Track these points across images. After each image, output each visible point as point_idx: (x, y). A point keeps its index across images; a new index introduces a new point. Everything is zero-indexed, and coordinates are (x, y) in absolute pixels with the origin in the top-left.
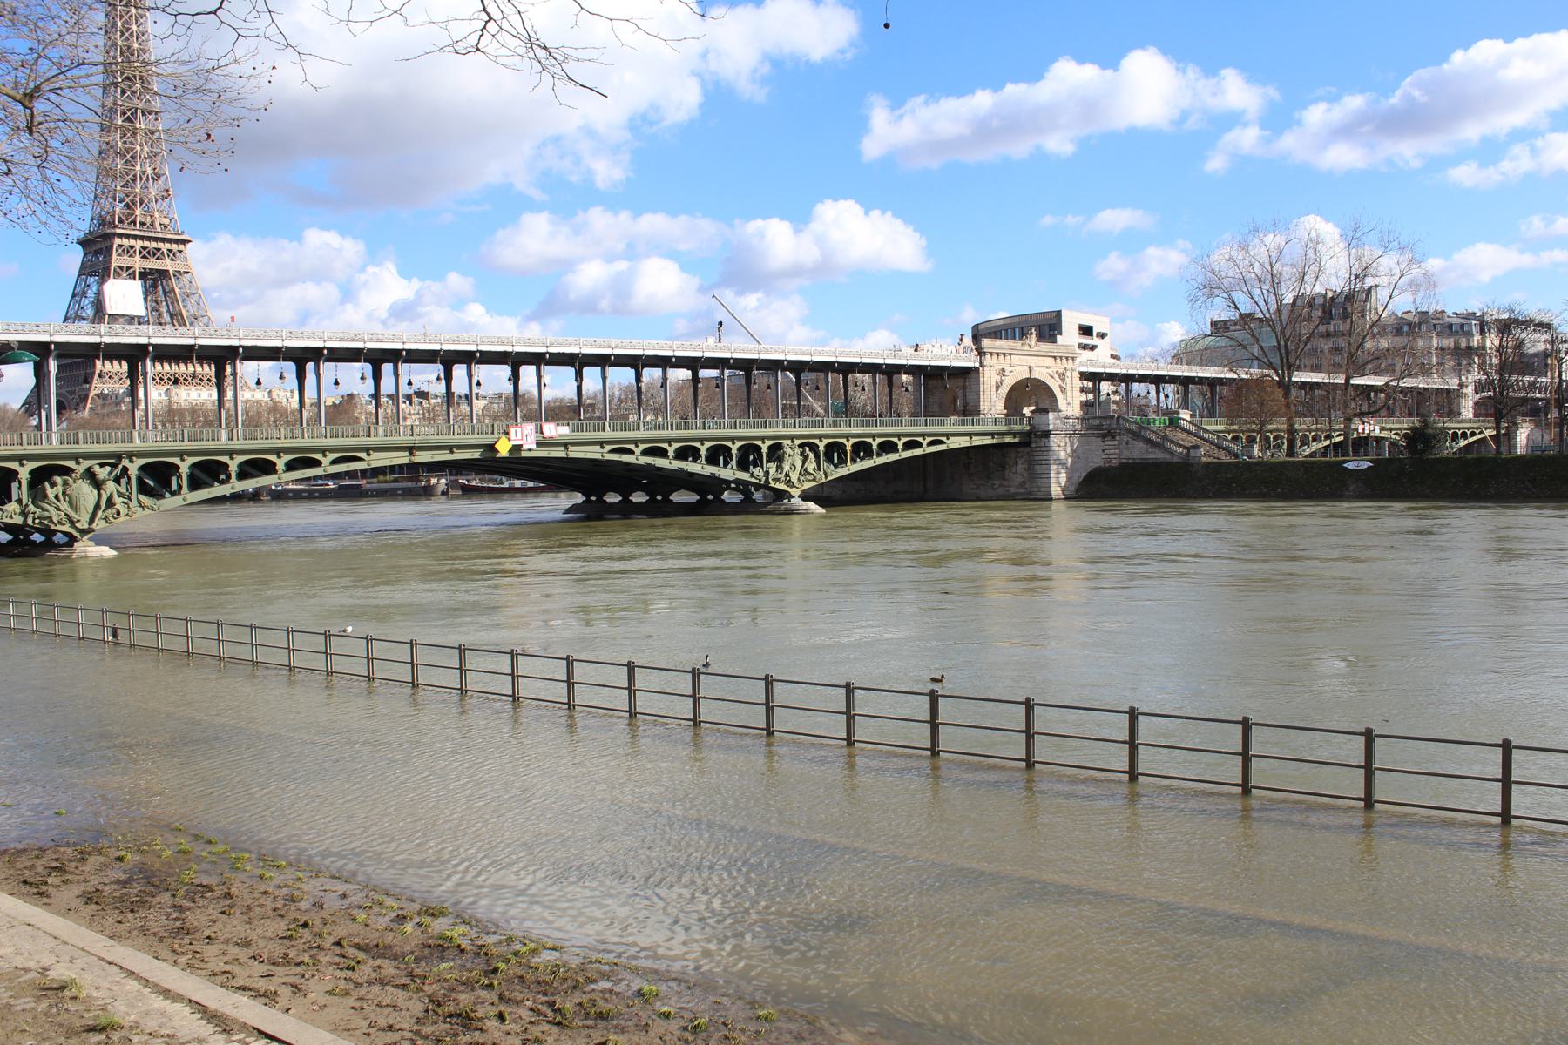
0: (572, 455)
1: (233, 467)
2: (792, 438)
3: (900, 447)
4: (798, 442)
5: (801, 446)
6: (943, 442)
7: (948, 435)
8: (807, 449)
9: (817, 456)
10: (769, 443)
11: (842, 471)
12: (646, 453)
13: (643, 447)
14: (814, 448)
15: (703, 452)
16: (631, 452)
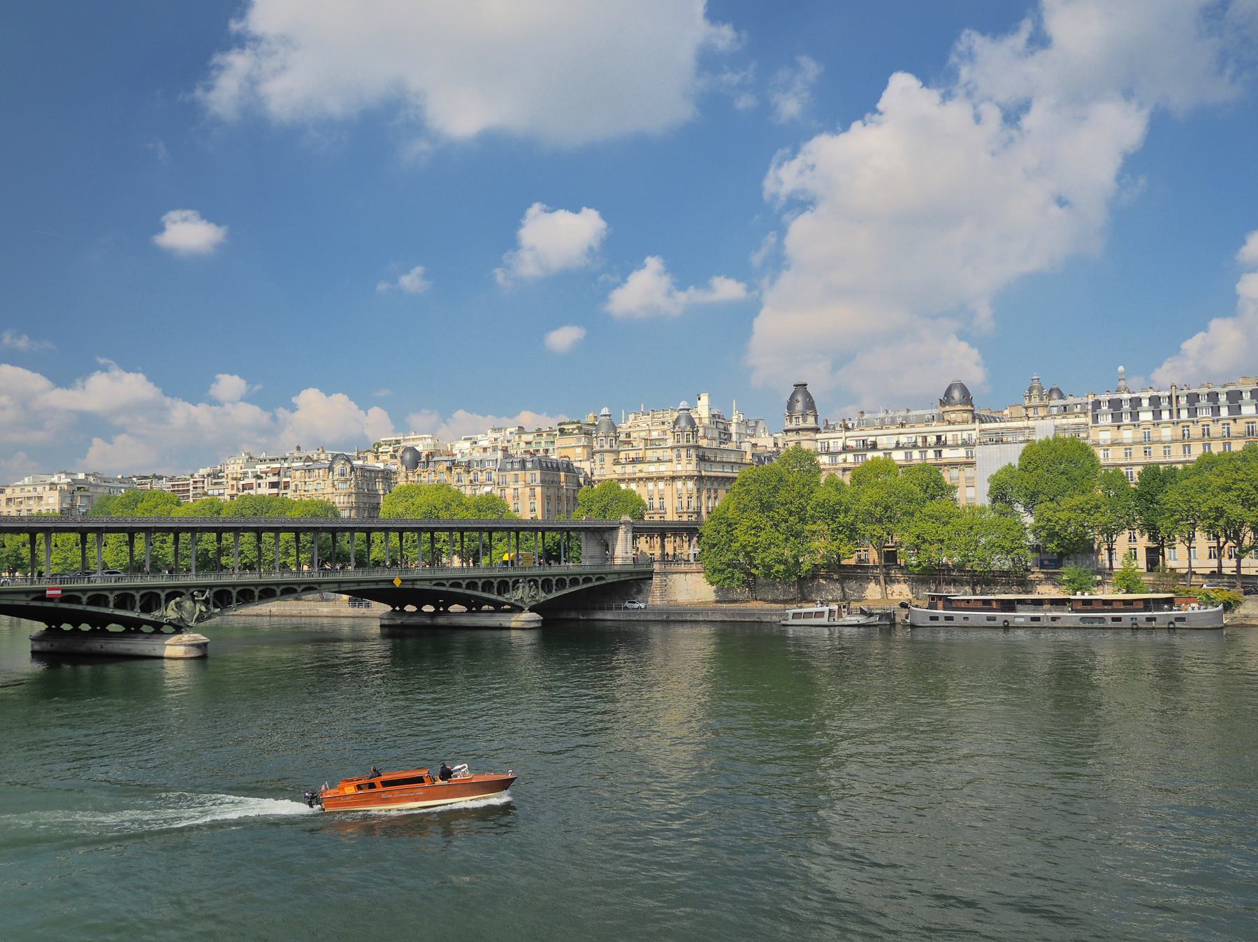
0: (416, 587)
1: (257, 593)
2: (525, 577)
3: (581, 581)
4: (528, 579)
5: (529, 582)
6: (603, 579)
7: (606, 574)
8: (532, 583)
9: (537, 588)
10: (513, 579)
11: (550, 597)
12: (451, 586)
13: (451, 582)
14: (536, 582)
15: (480, 585)
16: (444, 585)
